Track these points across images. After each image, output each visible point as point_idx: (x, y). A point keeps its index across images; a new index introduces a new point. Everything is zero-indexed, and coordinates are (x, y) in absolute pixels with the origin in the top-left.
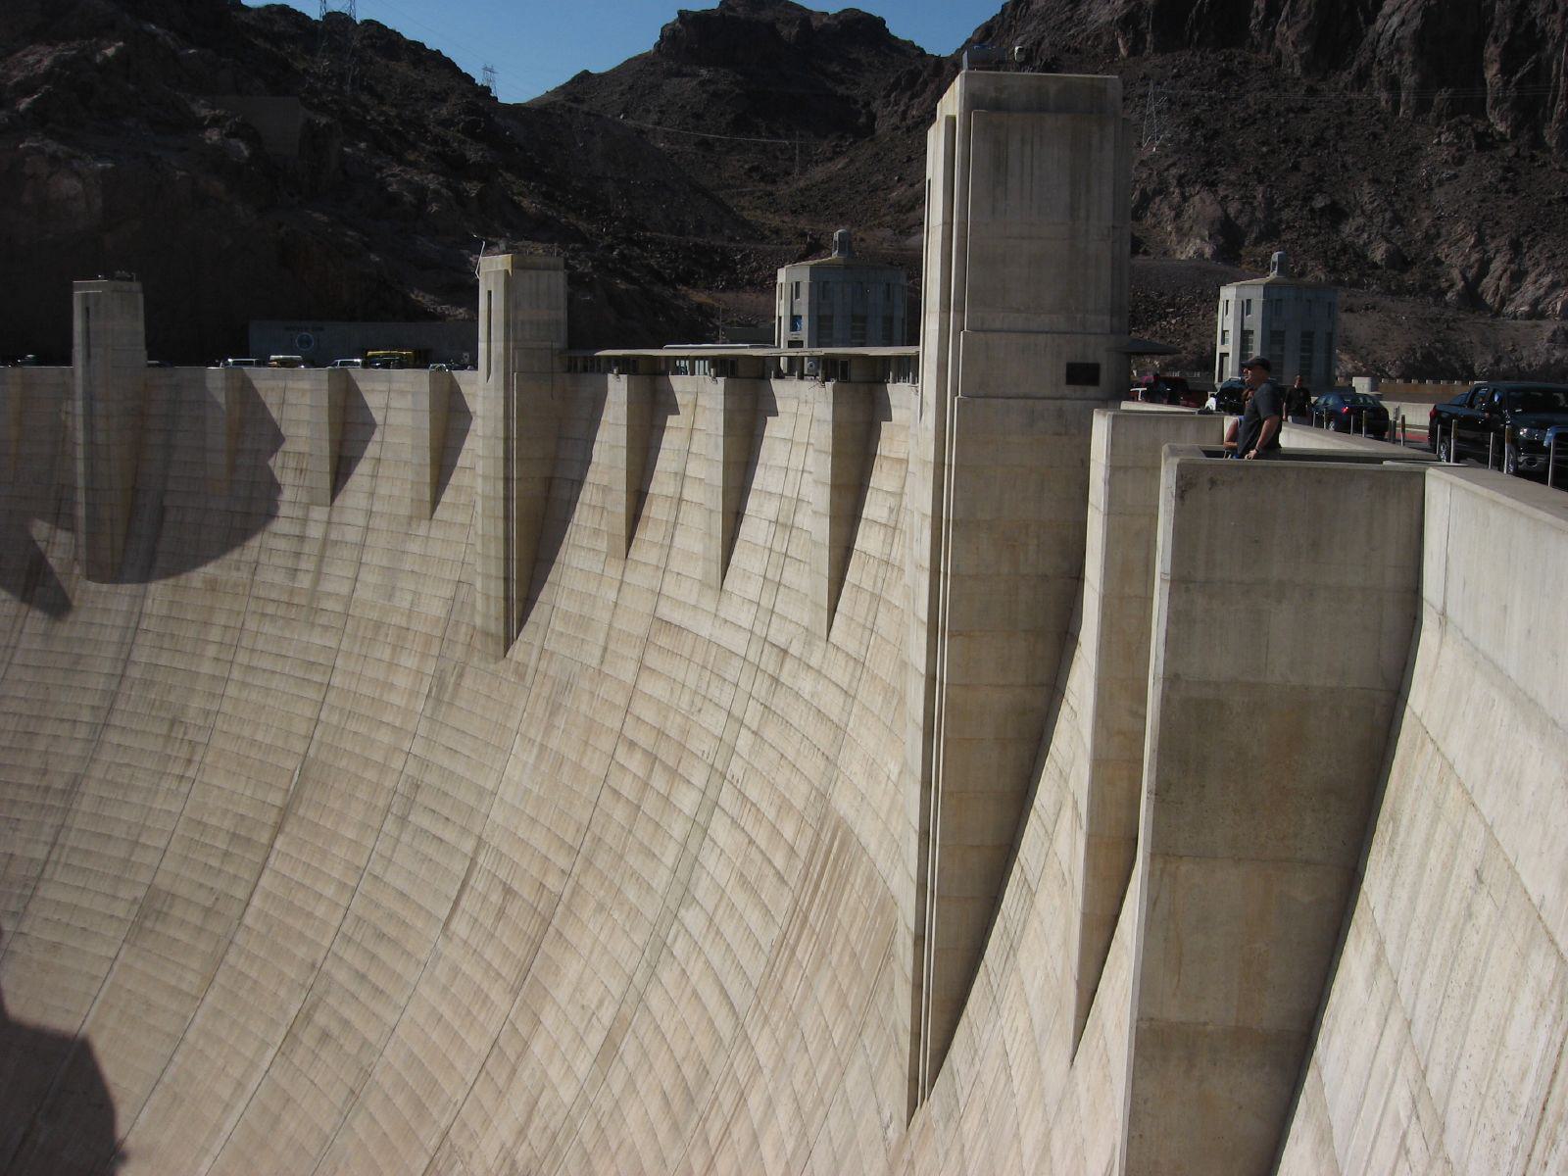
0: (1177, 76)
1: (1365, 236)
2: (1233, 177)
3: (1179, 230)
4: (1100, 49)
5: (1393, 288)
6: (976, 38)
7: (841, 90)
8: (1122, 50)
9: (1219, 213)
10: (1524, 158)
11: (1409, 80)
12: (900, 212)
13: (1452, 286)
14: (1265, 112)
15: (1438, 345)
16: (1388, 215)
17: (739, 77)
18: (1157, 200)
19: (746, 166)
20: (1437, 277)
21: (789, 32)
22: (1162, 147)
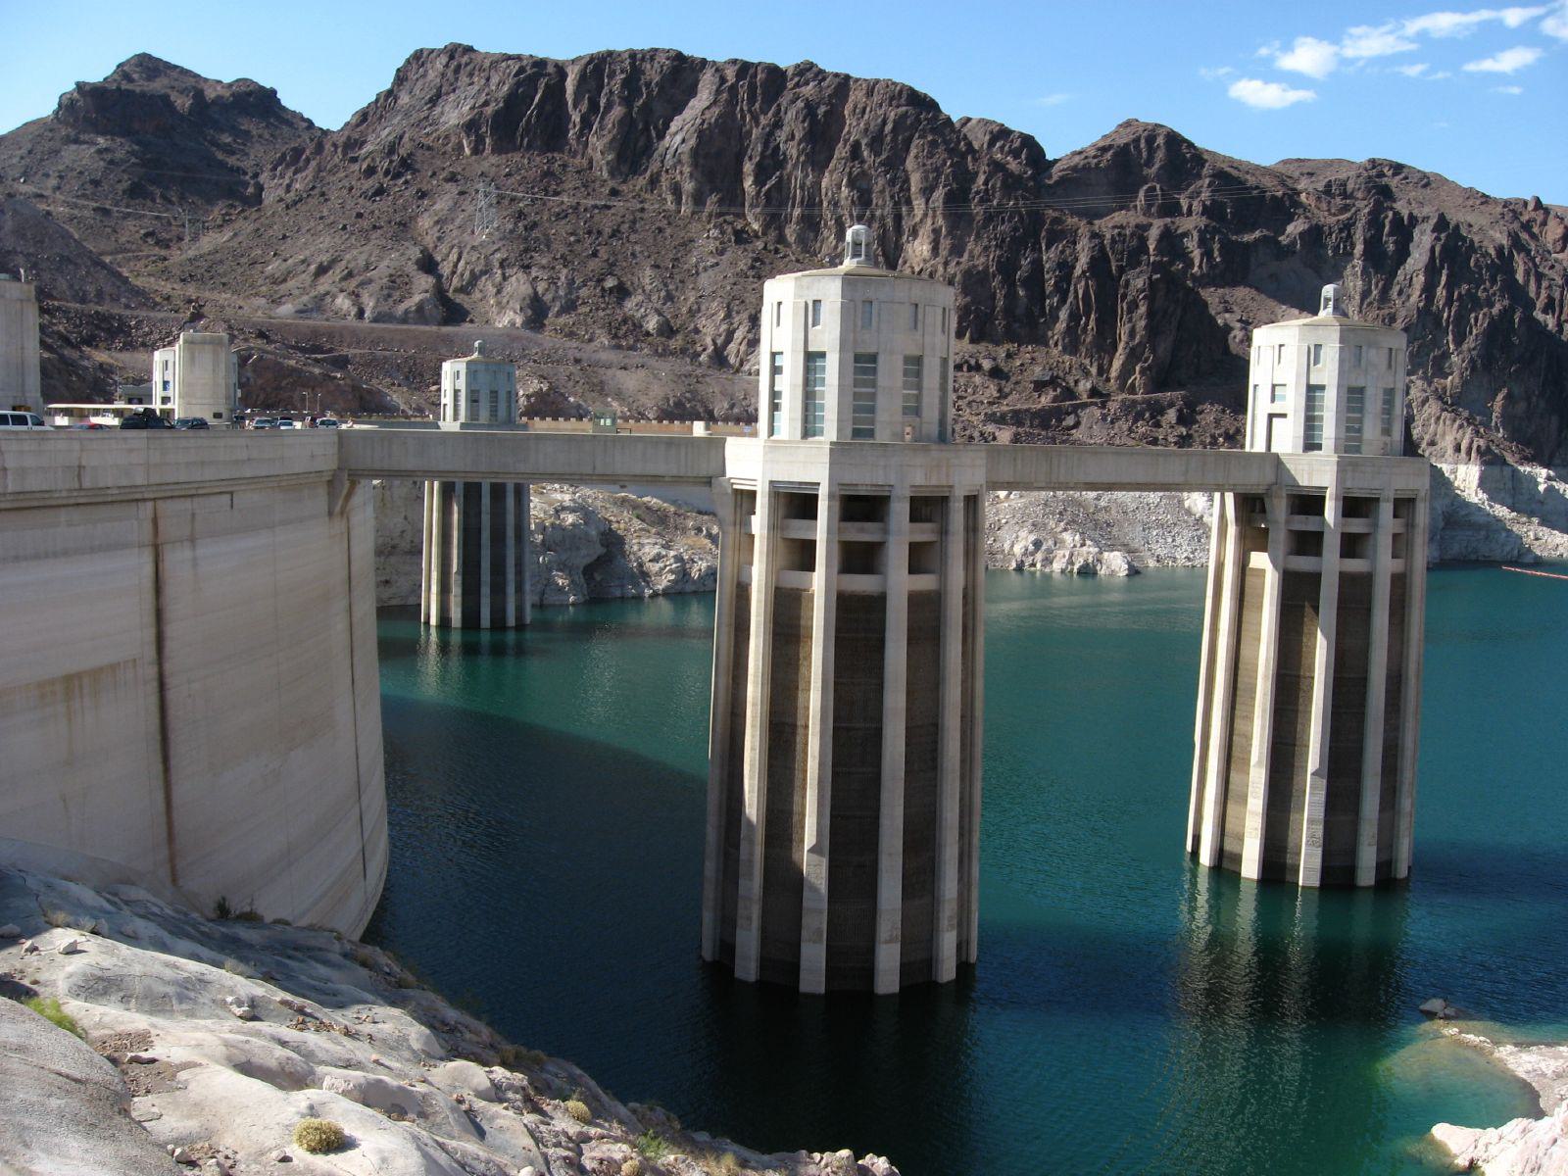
0: (508, 175)
1: (643, 310)
2: (544, 262)
3: (499, 303)
4: (449, 148)
5: (660, 351)
6: (354, 121)
7: (232, 161)
8: (466, 149)
9: (530, 291)
10: (770, 251)
11: (688, 186)
12: (274, 283)
13: (704, 350)
14: (576, 208)
15: (688, 395)
16: (663, 294)
17: (136, 148)
18: (484, 278)
19: (142, 232)
20: (694, 343)
21: (183, 103)
22: (490, 235)
